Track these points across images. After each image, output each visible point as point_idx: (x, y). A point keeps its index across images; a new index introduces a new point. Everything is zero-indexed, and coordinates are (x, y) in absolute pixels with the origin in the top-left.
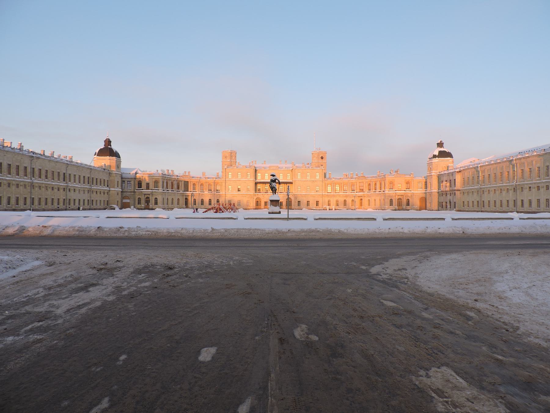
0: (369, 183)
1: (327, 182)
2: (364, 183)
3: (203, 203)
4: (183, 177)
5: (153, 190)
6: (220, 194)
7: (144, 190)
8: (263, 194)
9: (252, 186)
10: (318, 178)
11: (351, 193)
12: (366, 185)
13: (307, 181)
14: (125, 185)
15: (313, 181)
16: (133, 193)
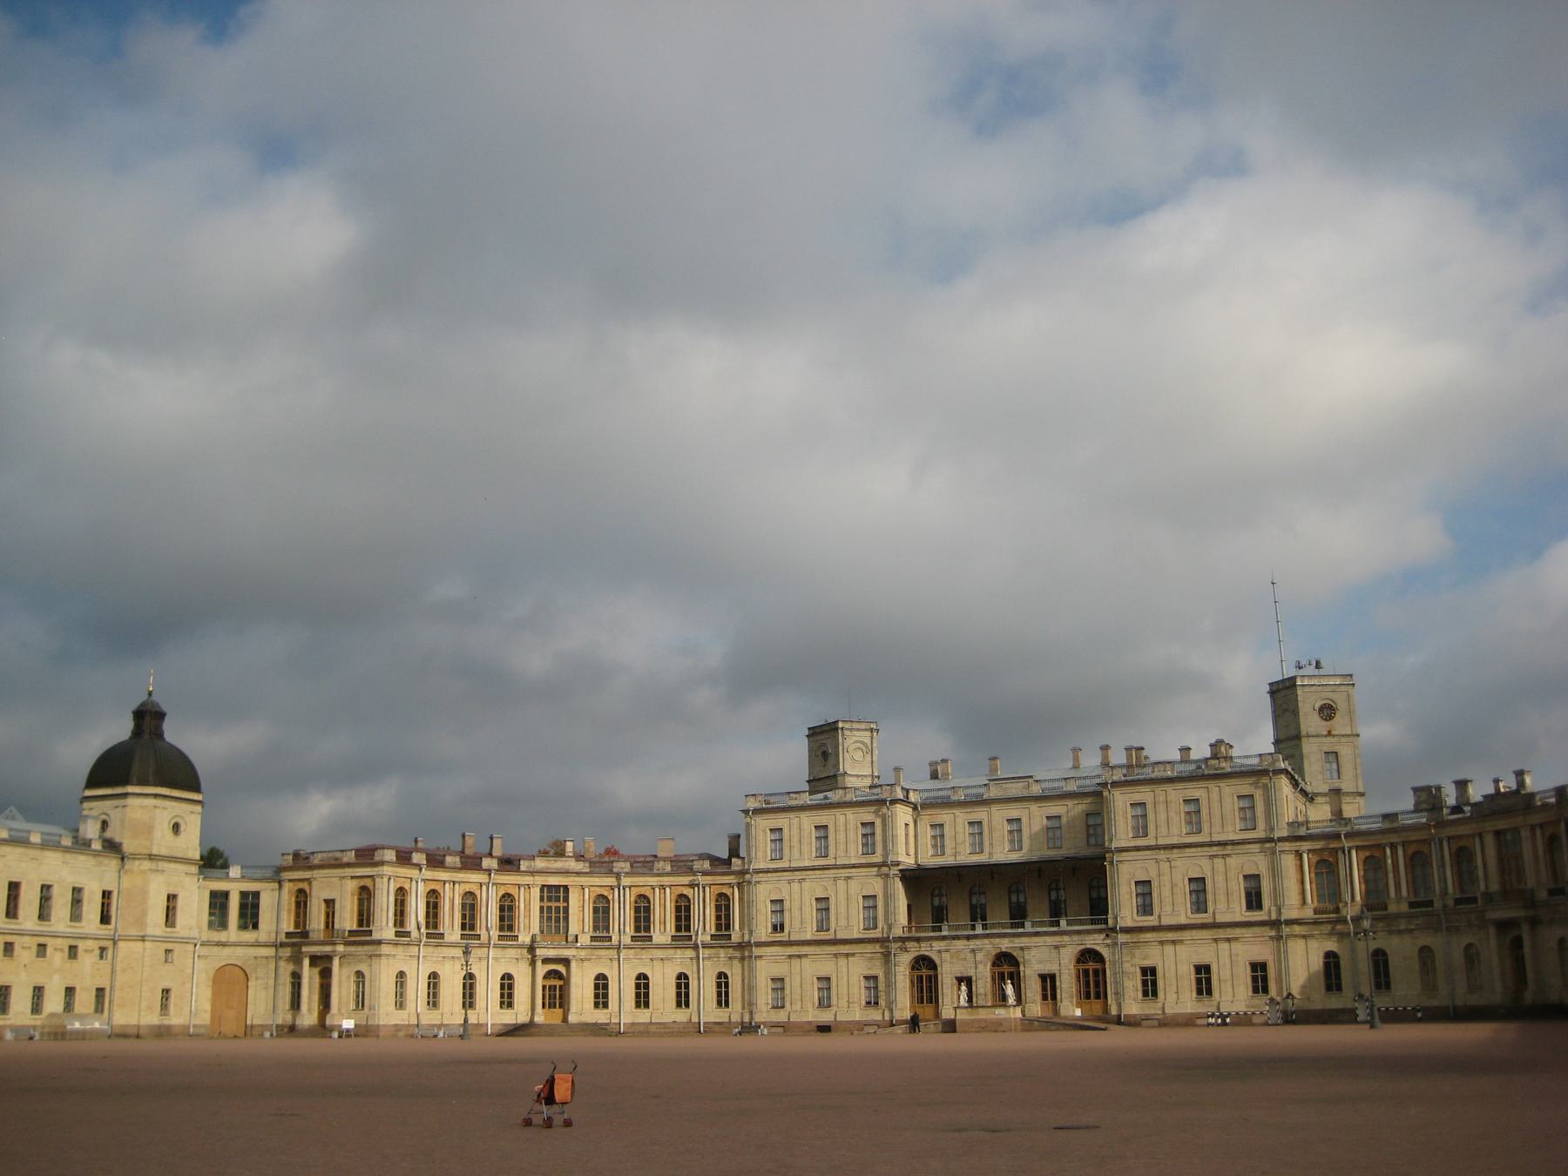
2: (1525, 833)
3: (647, 995)
12: (1535, 846)
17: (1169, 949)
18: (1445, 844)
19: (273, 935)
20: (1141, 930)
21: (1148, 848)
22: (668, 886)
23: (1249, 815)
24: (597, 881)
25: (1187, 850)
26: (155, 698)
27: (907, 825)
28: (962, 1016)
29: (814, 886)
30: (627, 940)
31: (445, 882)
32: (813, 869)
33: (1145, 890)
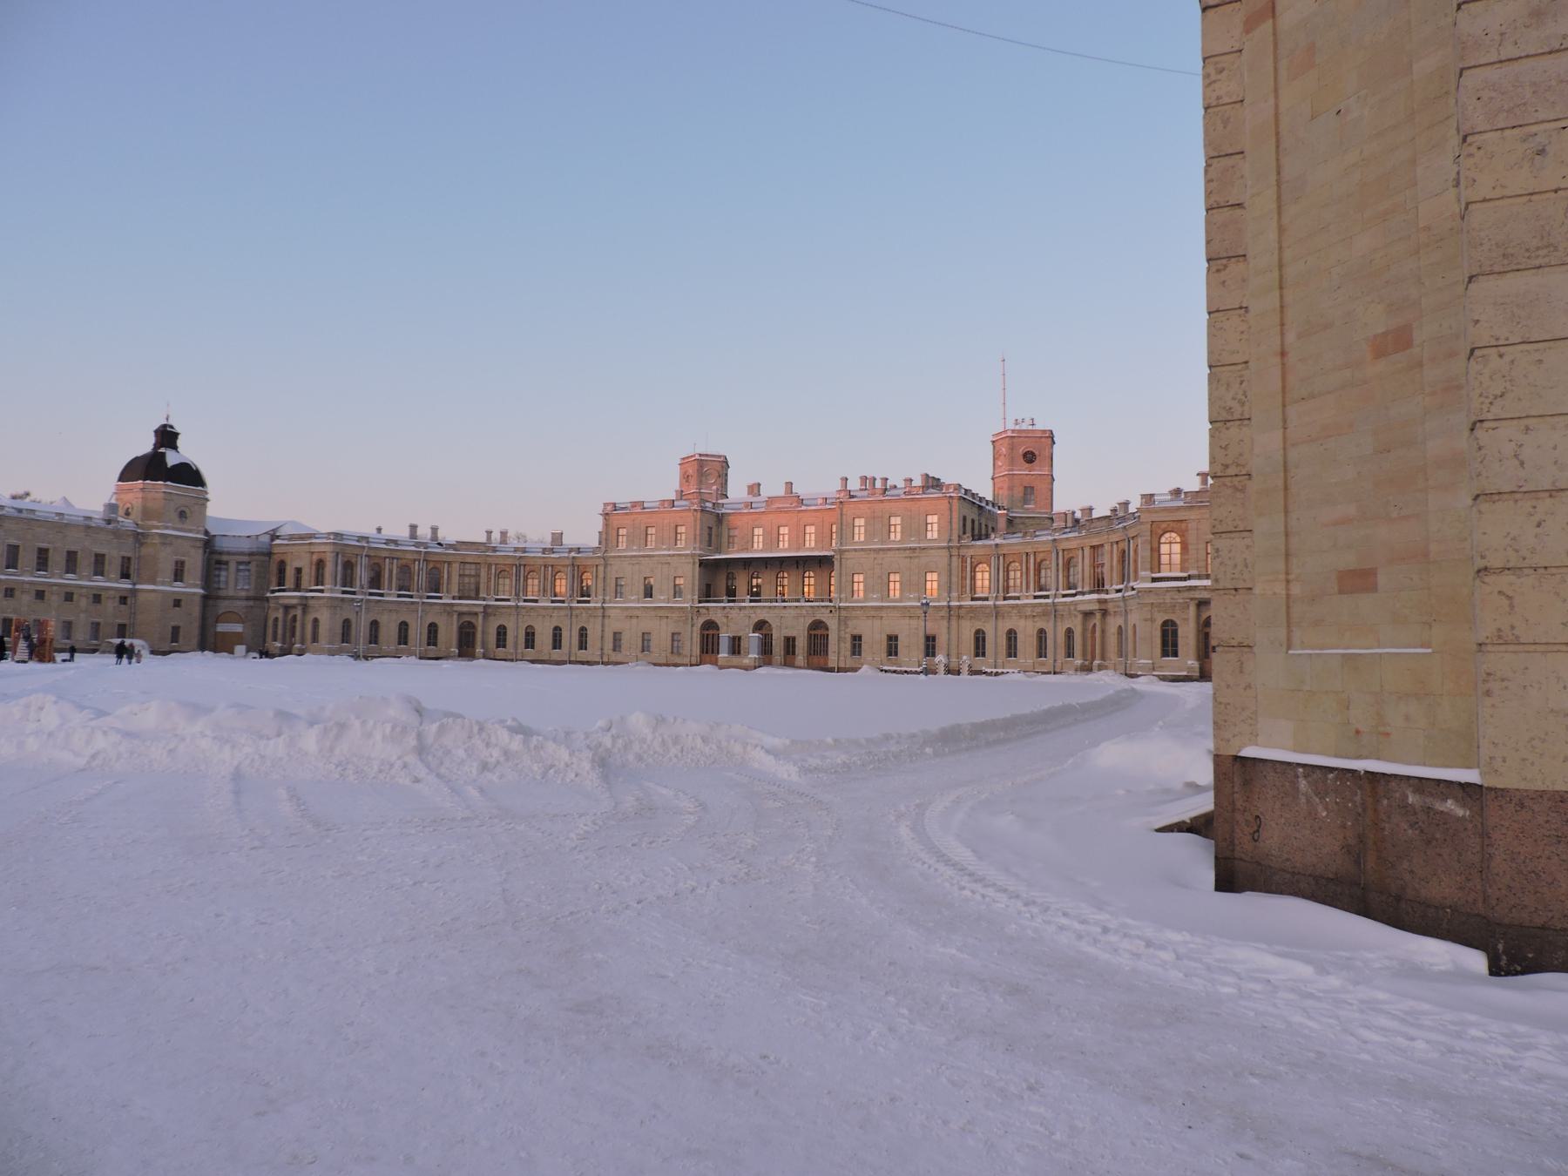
1: (971, 552)
2: (1107, 547)
3: (533, 641)
4: (458, 547)
5: (312, 591)
6: (589, 608)
7: (290, 590)
8: (724, 608)
9: (689, 577)
10: (933, 534)
11: (1064, 596)
13: (889, 549)
14: (227, 577)
15: (910, 548)
16: (251, 603)
18: (1060, 554)
22: (552, 566)
25: (889, 552)
27: (710, 528)
31: (385, 558)
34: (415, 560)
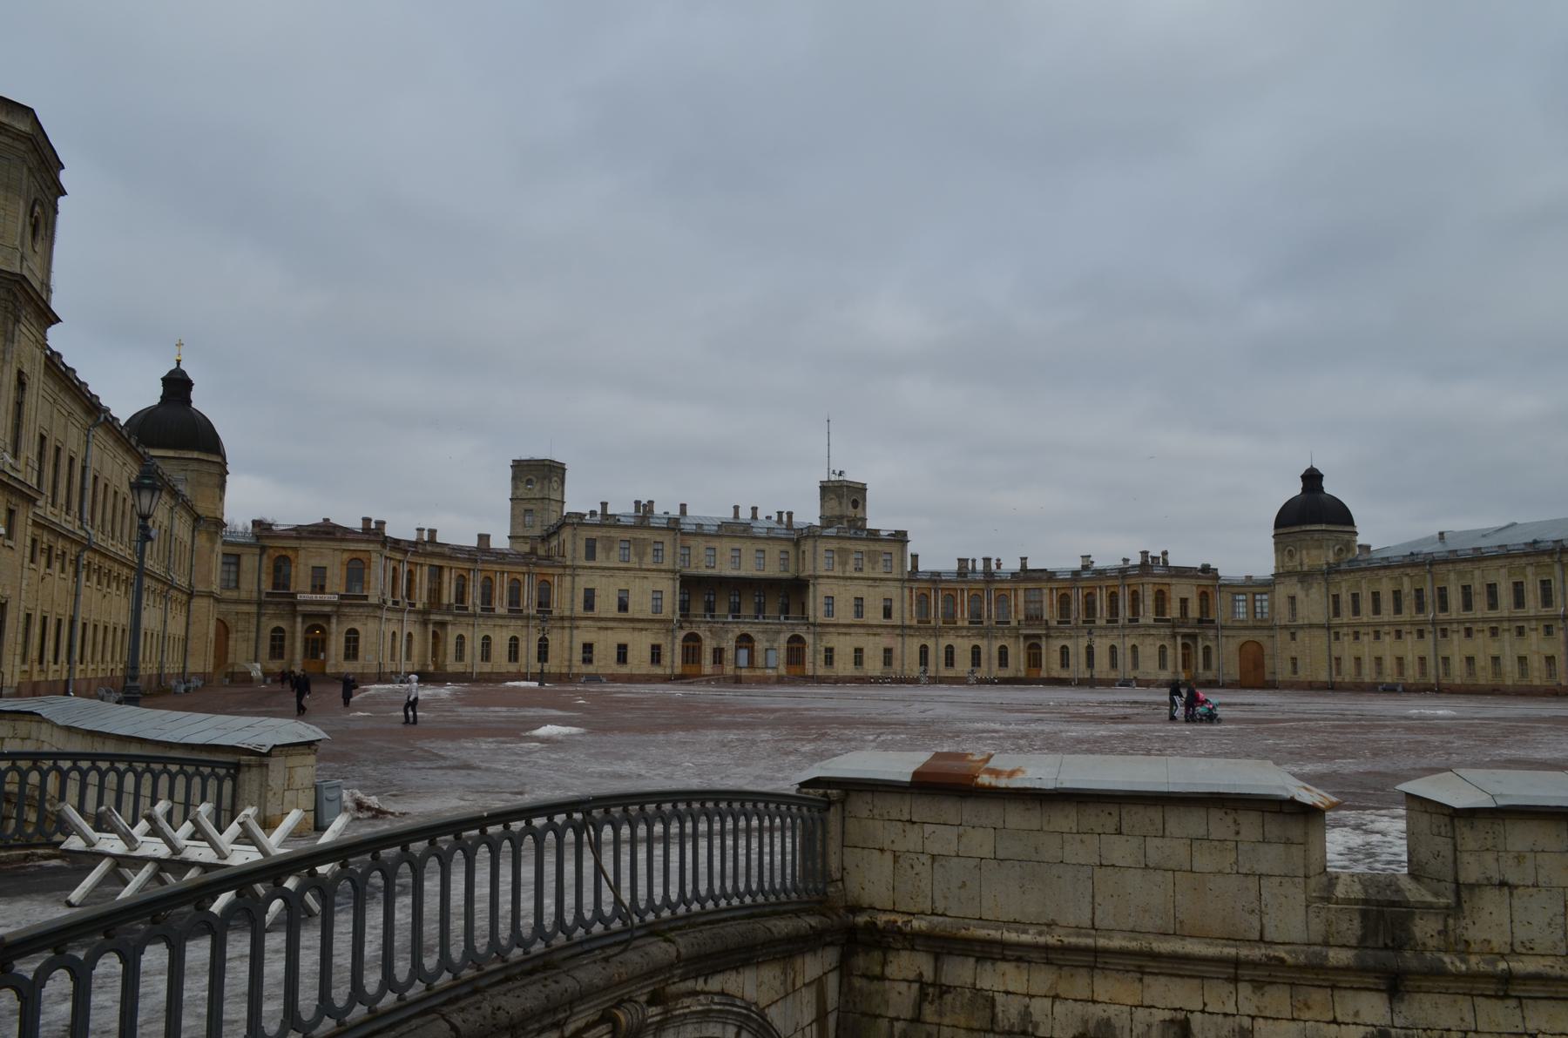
0: (1063, 591)
2: (1046, 591)
12: (1051, 600)
17: (842, 638)
19: (255, 595)
20: (828, 625)
21: (835, 577)
22: (508, 572)
23: (889, 564)
24: (460, 565)
26: (182, 367)
28: (744, 672)
29: (621, 582)
30: (479, 610)
32: (619, 569)
33: (830, 600)
34: (400, 561)
